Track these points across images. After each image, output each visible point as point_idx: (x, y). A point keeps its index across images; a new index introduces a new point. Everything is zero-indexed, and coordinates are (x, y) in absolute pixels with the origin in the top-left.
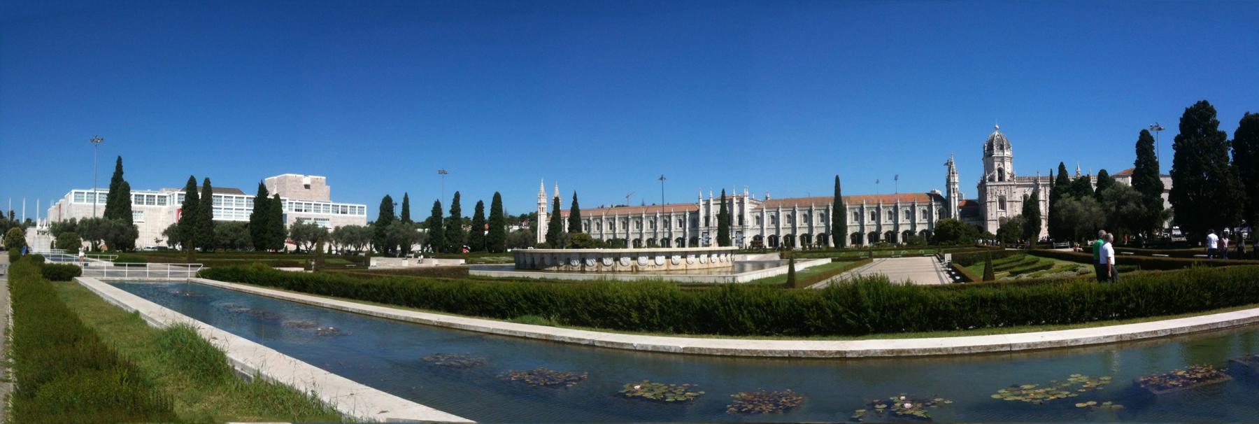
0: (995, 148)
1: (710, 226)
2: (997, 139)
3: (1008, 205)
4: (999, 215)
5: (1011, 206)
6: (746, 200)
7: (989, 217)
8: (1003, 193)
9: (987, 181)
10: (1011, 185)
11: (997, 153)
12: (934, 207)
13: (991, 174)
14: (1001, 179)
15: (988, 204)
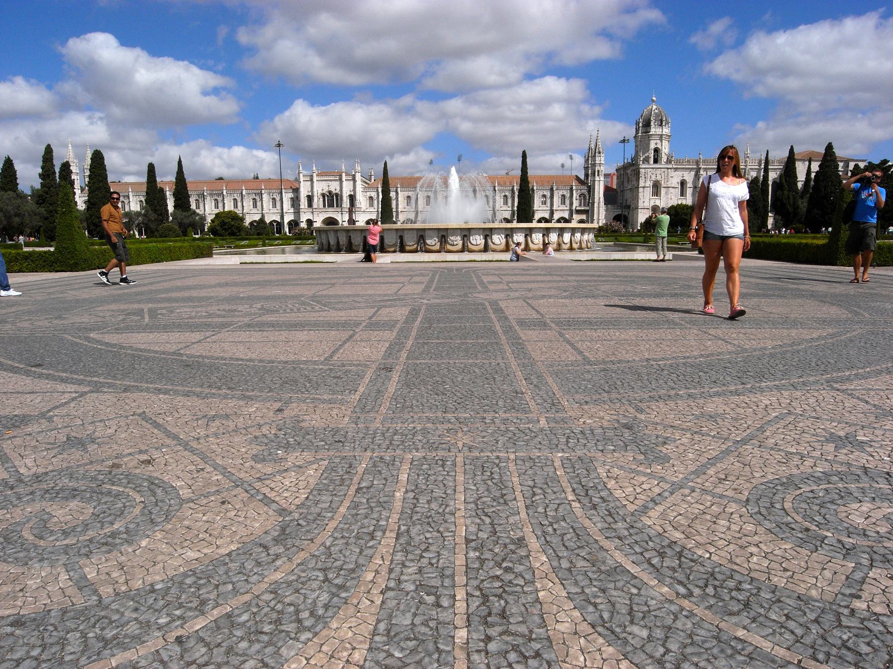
0: (652, 123)
1: (315, 206)
2: (655, 113)
3: (663, 191)
4: (652, 204)
5: (666, 193)
6: (358, 177)
7: (641, 205)
8: (659, 178)
9: (641, 162)
10: (668, 168)
11: (654, 130)
12: (574, 191)
13: (647, 155)
14: (656, 161)
15: (641, 190)
